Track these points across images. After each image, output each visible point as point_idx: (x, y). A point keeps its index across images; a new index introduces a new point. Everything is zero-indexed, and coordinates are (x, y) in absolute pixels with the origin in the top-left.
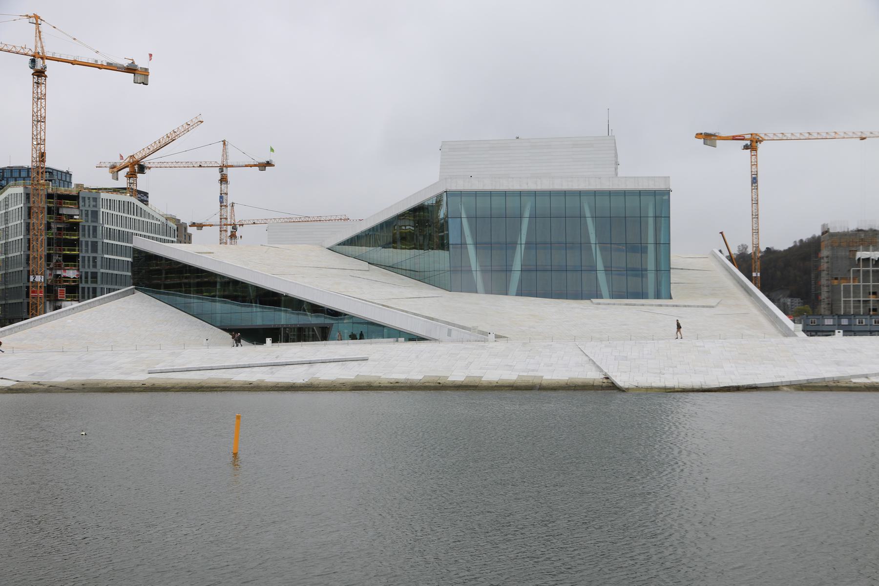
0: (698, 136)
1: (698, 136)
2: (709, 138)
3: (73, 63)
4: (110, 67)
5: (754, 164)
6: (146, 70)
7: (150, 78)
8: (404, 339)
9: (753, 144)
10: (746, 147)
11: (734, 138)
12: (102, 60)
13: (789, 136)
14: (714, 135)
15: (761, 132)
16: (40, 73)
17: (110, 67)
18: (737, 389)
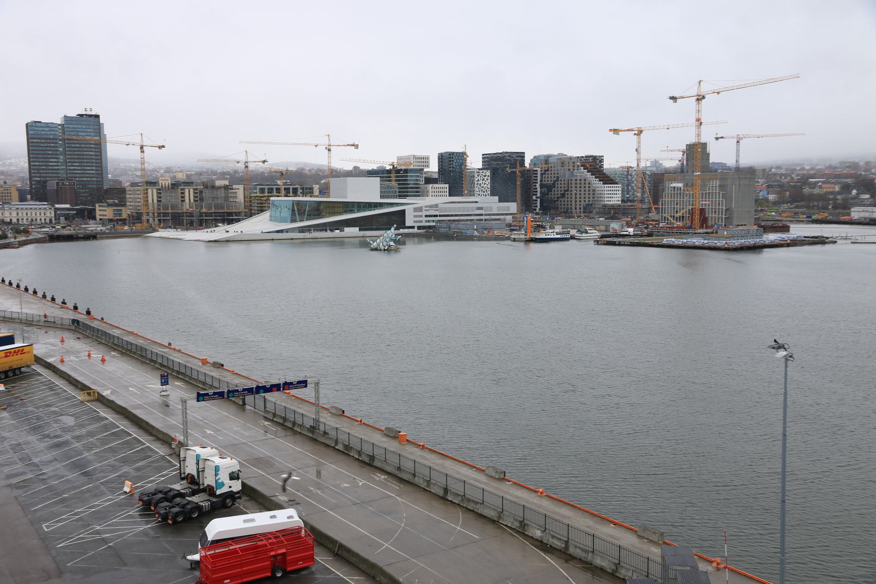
0: (611, 130)
1: (611, 130)
2: (616, 131)
3: (338, 146)
4: (348, 145)
5: (639, 142)
6: (358, 145)
7: (359, 147)
8: (358, 228)
9: (640, 132)
10: (635, 134)
11: (628, 130)
12: (346, 144)
13: (657, 128)
14: (618, 130)
15: (642, 126)
16: (329, 150)
17: (348, 145)
18: (215, 241)
